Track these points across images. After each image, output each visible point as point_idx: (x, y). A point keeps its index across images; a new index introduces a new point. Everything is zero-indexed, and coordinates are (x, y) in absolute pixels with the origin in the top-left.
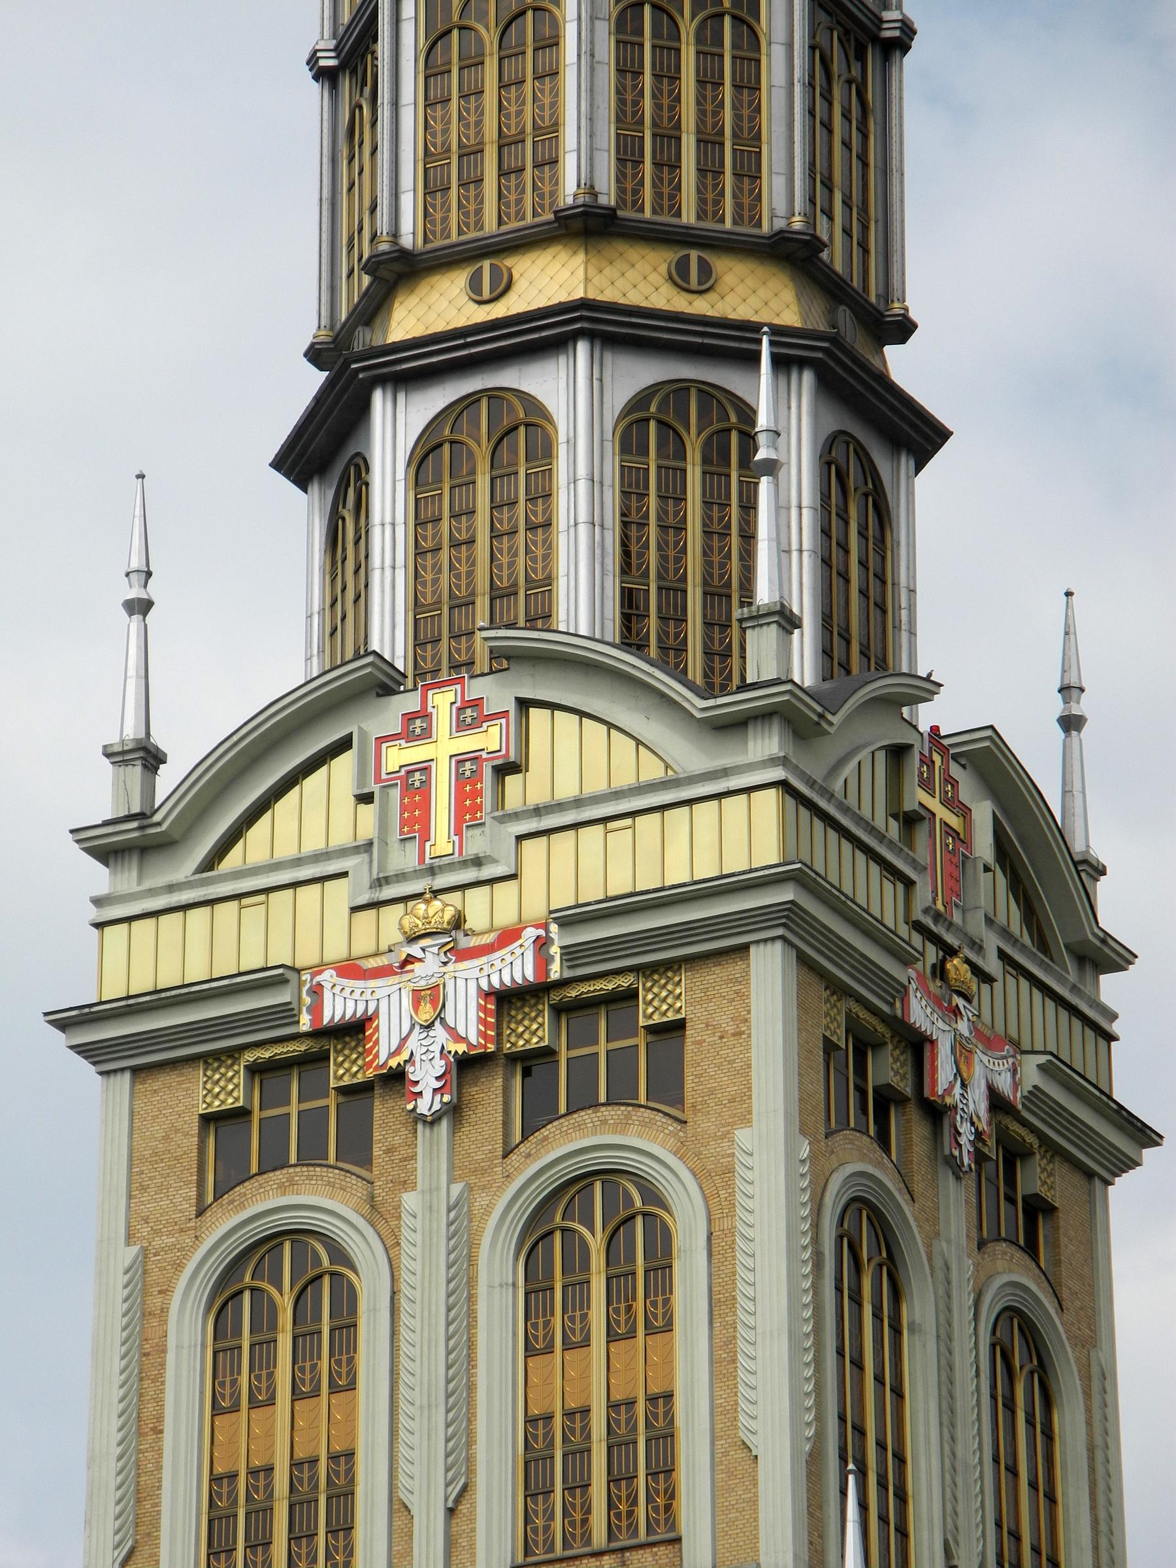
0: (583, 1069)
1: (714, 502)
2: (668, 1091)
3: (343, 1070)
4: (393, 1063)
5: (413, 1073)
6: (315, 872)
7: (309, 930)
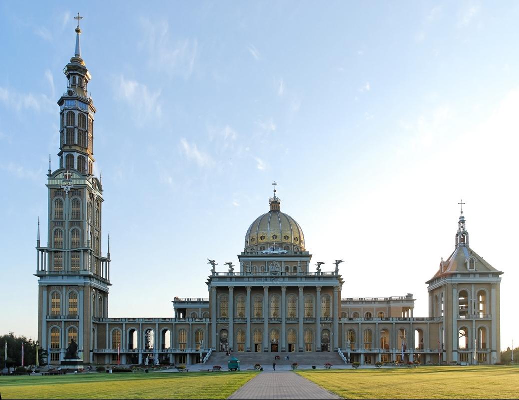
0: (75, 194)
1: (83, 163)
2: (80, 195)
6: (61, 179)
7: (60, 183)
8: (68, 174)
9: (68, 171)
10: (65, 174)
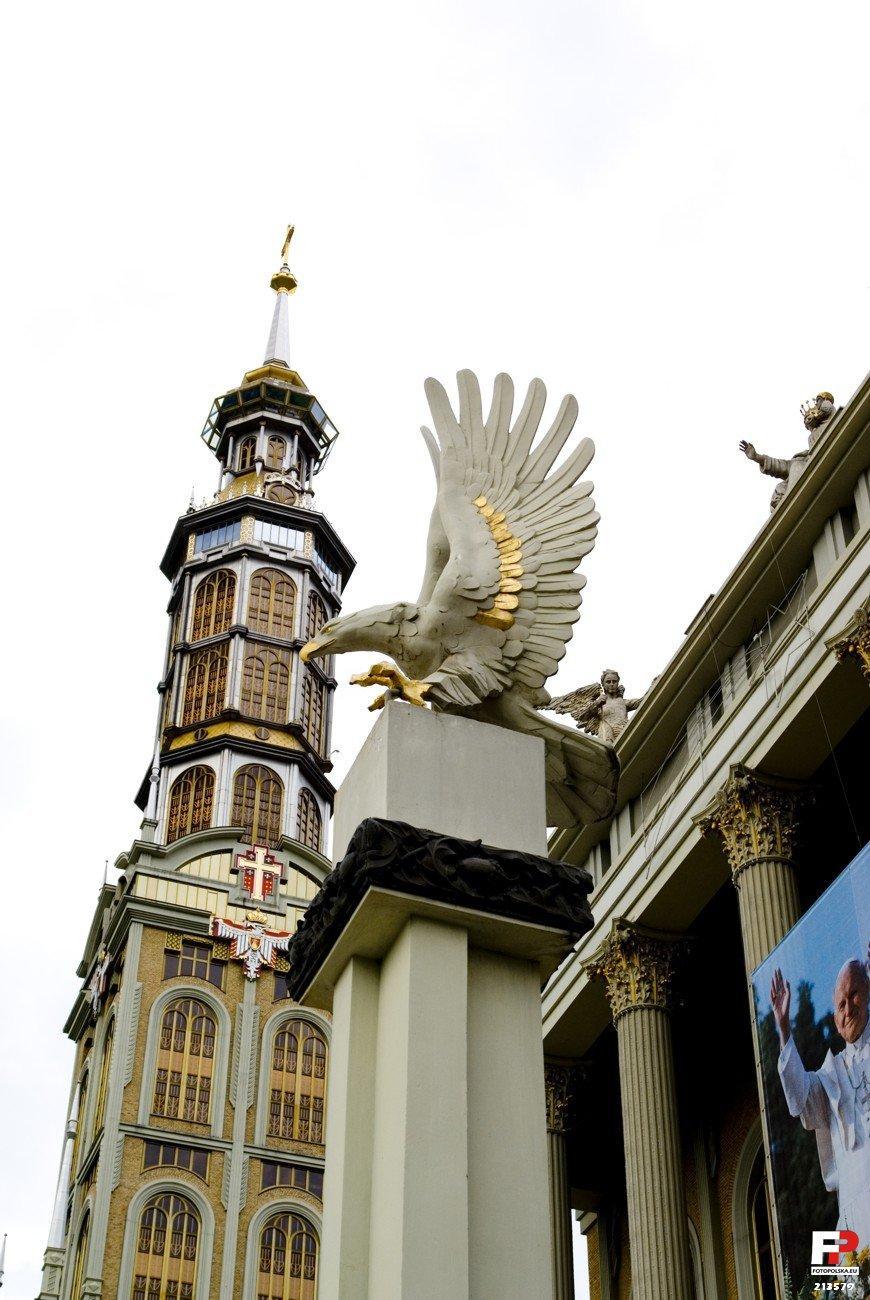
3: (217, 952)
4: (241, 957)
5: (248, 963)
8: (259, 866)
9: (261, 853)
10: (243, 863)
